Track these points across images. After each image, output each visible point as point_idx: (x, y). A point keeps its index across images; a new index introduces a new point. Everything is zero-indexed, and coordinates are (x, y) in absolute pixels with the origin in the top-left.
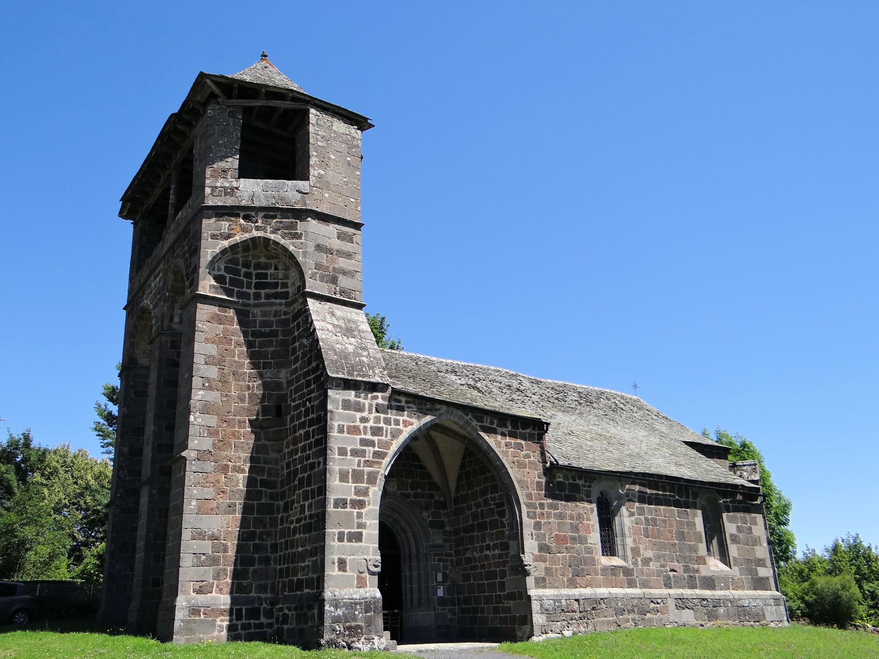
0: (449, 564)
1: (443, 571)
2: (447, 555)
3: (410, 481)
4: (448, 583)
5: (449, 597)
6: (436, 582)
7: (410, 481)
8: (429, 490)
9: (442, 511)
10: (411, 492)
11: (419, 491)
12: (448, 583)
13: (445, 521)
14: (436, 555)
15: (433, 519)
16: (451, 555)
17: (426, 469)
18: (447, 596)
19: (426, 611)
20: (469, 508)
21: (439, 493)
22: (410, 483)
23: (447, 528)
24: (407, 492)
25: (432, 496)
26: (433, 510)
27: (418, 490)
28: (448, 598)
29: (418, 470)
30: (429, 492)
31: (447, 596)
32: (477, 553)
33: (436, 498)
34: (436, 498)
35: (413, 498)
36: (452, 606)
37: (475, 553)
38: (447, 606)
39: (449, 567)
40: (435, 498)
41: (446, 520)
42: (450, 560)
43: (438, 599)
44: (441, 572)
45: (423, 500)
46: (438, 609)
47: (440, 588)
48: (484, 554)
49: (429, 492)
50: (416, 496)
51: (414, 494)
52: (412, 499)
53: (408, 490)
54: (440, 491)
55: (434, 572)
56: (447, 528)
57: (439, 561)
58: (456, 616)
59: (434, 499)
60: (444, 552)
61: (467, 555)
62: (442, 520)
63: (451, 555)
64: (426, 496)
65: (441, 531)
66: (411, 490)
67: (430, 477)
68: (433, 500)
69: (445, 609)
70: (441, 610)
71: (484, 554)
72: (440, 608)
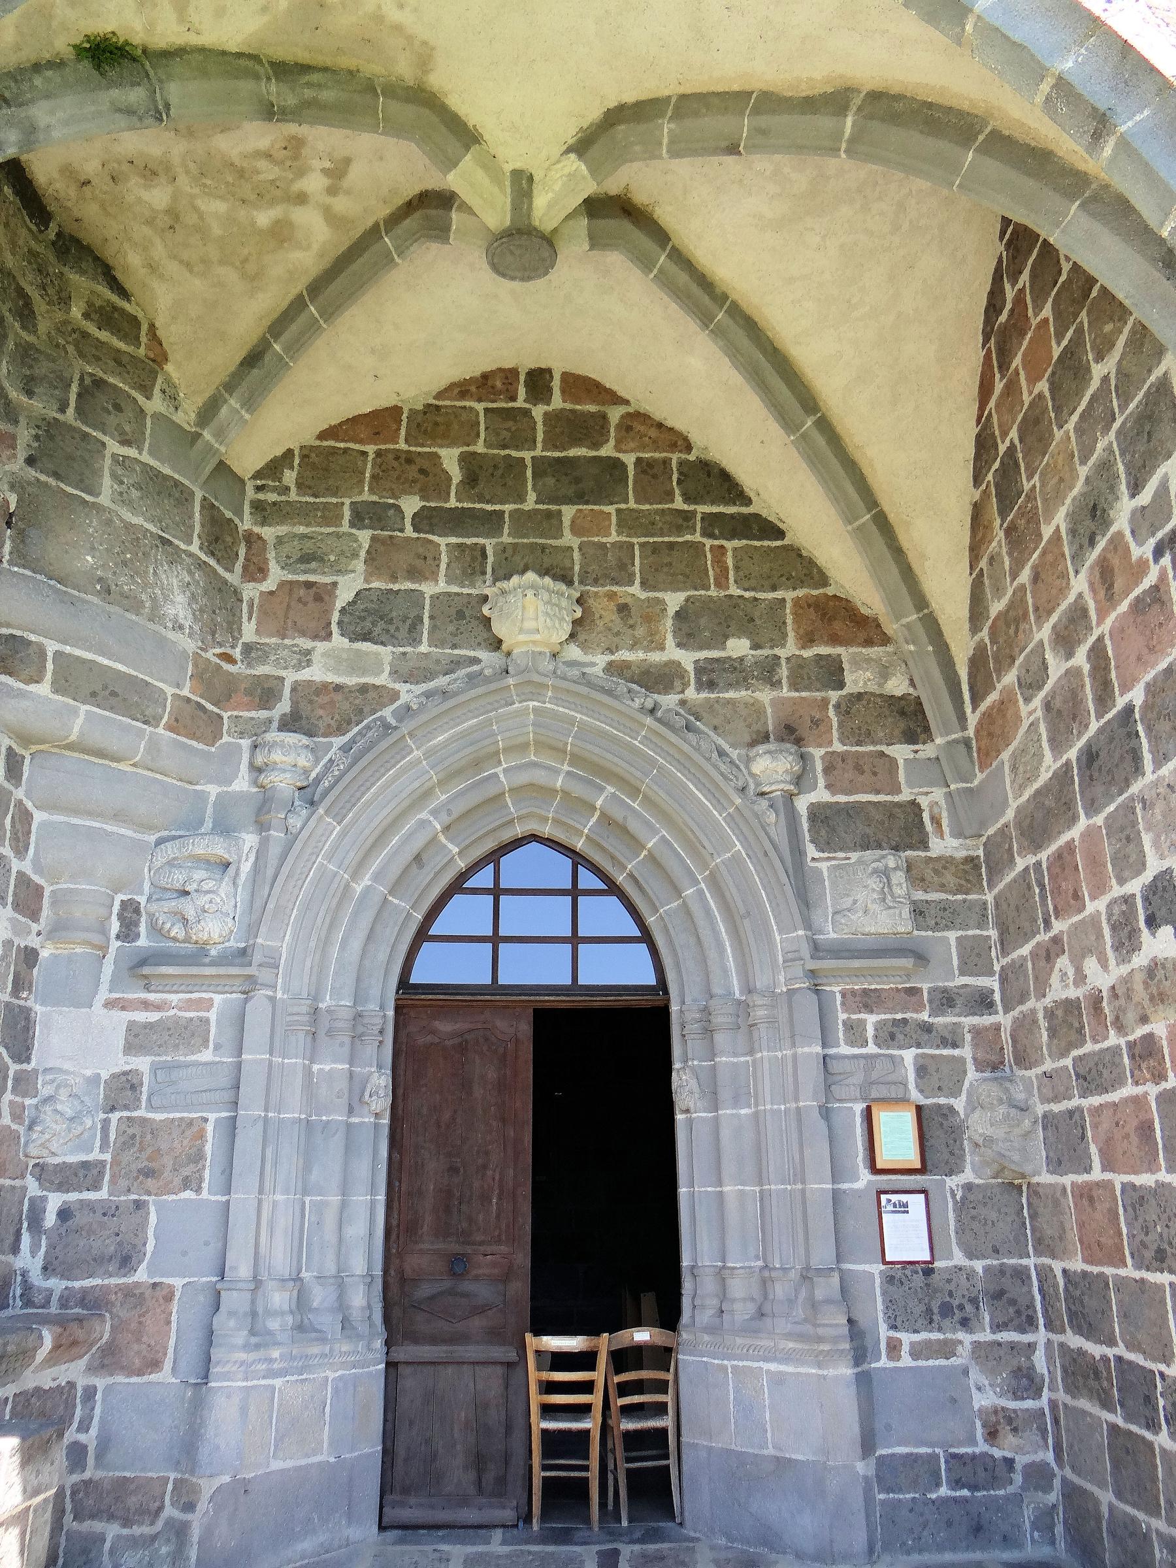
0: (966, 1052)
1: (923, 1101)
2: (946, 1000)
3: (674, 600)
4: (968, 1175)
5: (978, 1266)
6: (875, 1170)
7: (674, 600)
8: (808, 640)
9: (901, 752)
10: (687, 659)
11: (738, 647)
12: (968, 1175)
13: (924, 802)
14: (868, 1000)
15: (842, 799)
16: (983, 1003)
17: (780, 534)
18: (959, 1258)
19: (787, 1358)
20: (1031, 684)
21: (875, 651)
22: (672, 609)
23: (944, 845)
24: (656, 657)
25: (833, 674)
26: (838, 747)
27: (731, 643)
28: (971, 1275)
29: (729, 545)
30: (807, 653)
31: (959, 1258)
32: (1104, 964)
33: (857, 680)
34: (857, 680)
35: (700, 687)
36: (997, 1327)
37: (1091, 965)
38: (965, 1323)
39: (972, 1074)
40: (849, 677)
41: (932, 798)
42: (977, 1032)
43: (890, 1280)
44: (901, 1101)
45: (765, 696)
46: (894, 1348)
47: (903, 1208)
48: (1140, 960)
49: (807, 653)
50: (708, 675)
51: (701, 669)
52: (691, 693)
53: (663, 649)
54: (885, 640)
55: (859, 1107)
56: (944, 845)
57: (890, 1035)
58: (1038, 1394)
59: (841, 685)
60: (925, 987)
61: (1060, 990)
62: (905, 796)
63: (983, 1003)
64: (784, 672)
65: (891, 862)
66: (679, 645)
67: (812, 573)
68: (834, 696)
69: (947, 1349)
70: (915, 1354)
71: (1140, 960)
72: (906, 1338)
